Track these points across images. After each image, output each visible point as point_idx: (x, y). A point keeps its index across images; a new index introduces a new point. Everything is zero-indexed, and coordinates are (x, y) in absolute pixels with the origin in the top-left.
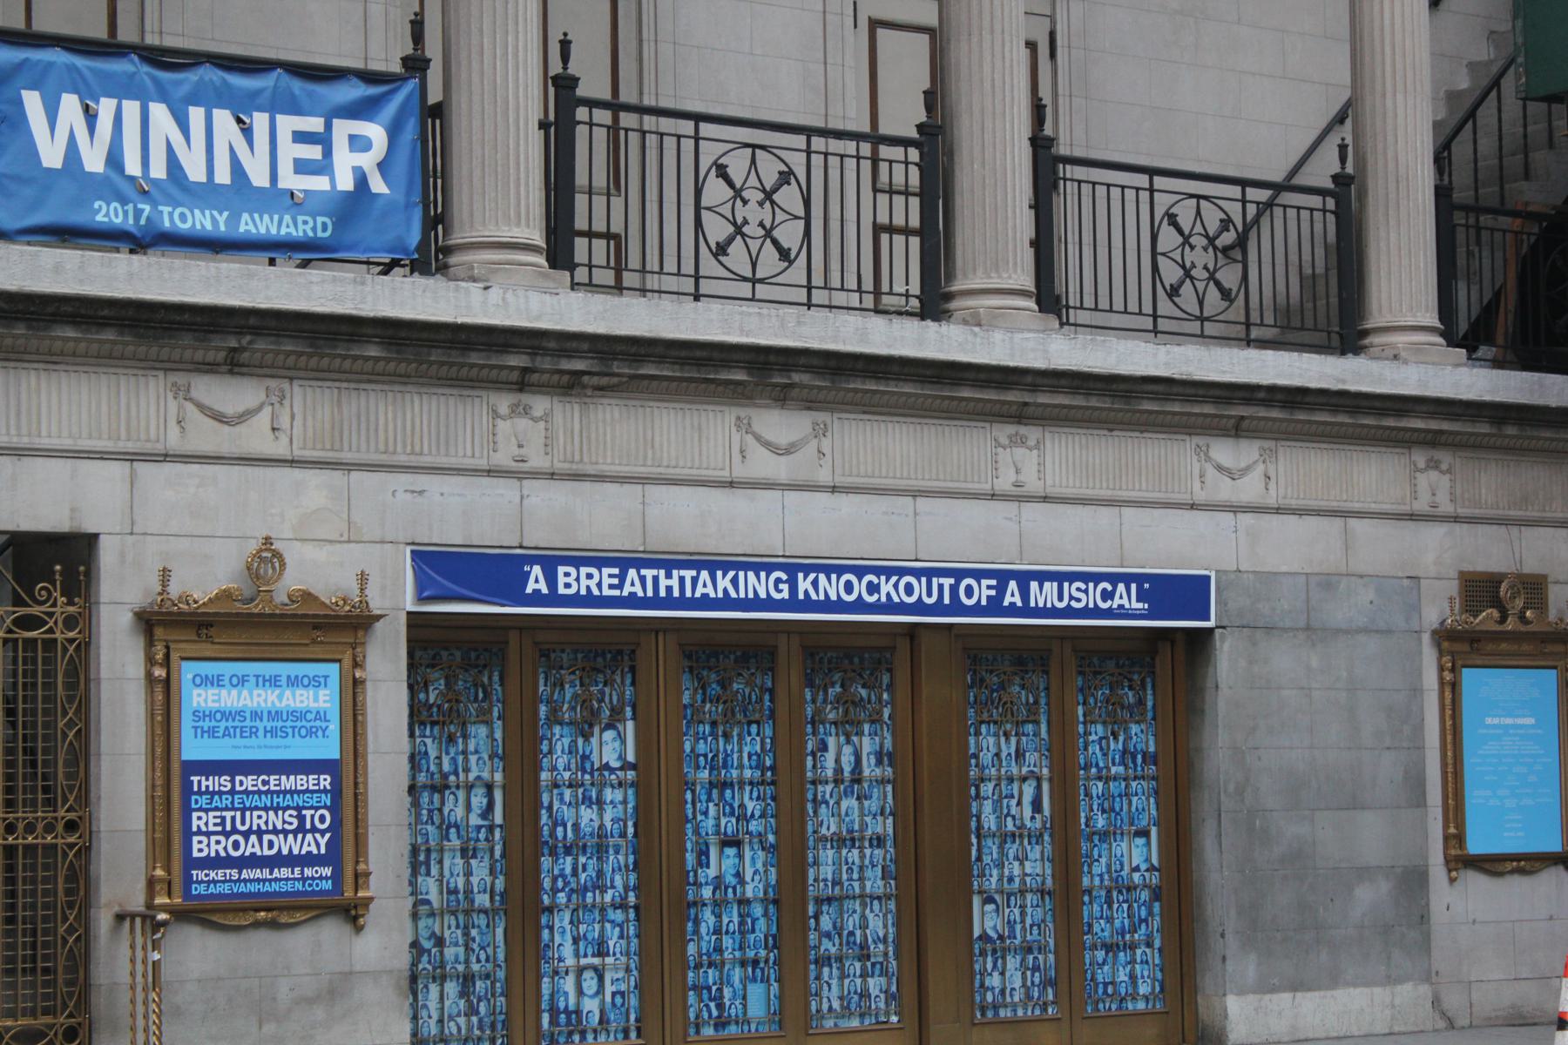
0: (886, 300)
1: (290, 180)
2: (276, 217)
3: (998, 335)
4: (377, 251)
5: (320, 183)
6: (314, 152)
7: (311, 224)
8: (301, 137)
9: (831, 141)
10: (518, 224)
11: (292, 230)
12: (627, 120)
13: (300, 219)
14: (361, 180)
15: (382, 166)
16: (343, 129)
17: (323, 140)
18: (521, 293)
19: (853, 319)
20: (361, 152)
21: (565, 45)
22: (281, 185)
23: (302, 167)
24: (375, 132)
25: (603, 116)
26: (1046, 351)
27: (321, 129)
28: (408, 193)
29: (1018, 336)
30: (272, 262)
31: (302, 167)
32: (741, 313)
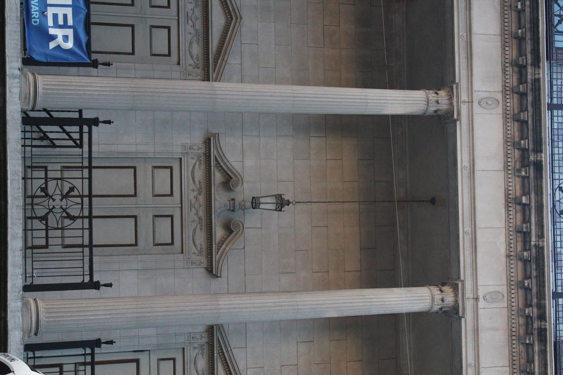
0: (29, 170)
1: (50, 11)
2: (37, 4)
3: (19, 304)
4: (29, 43)
5: (50, 23)
6: (61, 22)
7: (36, 17)
8: (65, 16)
9: (88, 258)
10: (43, 89)
11: (32, 10)
12: (86, 171)
13: (38, 13)
14: (53, 38)
15: (59, 46)
16: (70, 32)
17: (65, 26)
18: (19, 85)
19: (20, 271)
20: (63, 39)
21: (108, 64)
22: (48, 8)
23: (55, 16)
24: (70, 45)
25: (89, 359)
26: (15, 329)
27: (69, 24)
28: (50, 56)
29: (19, 314)
30: (21, 4)
31: (55, 16)
32: (19, 180)
